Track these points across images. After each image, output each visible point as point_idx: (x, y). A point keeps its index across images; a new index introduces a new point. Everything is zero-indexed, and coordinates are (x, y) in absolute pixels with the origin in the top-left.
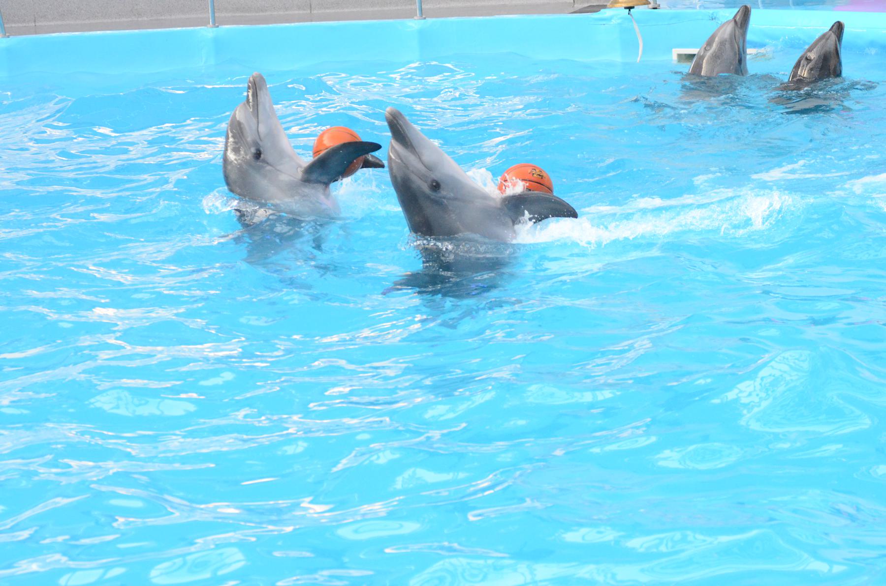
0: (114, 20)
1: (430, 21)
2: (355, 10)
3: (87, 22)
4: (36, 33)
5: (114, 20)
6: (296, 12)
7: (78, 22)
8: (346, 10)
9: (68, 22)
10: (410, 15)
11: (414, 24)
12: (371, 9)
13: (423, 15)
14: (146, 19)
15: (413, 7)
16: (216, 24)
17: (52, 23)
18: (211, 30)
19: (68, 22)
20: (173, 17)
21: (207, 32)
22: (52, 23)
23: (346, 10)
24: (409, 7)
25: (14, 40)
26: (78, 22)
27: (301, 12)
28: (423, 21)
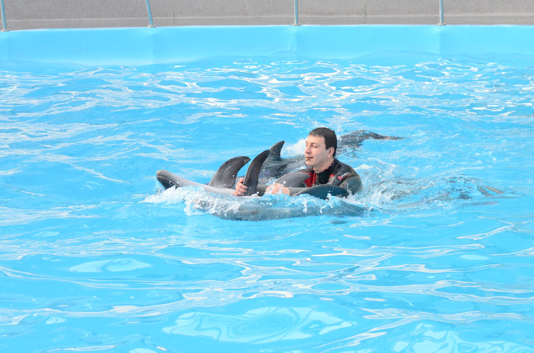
0: (228, 17)
1: (448, 26)
2: (396, 16)
3: (210, 17)
4: (174, 24)
5: (228, 17)
6: (355, 16)
7: (204, 17)
8: (390, 16)
9: (196, 17)
10: (434, 21)
11: (436, 29)
12: (407, 16)
13: (444, 23)
14: (250, 17)
15: (437, 15)
16: (299, 22)
17: (186, 18)
18: (295, 27)
19: (196, 17)
20: (269, 16)
21: (292, 29)
22: (186, 18)
23: (390, 16)
24: (434, 15)
25: (159, 30)
26: (204, 17)
27: (358, 16)
28: (444, 27)
